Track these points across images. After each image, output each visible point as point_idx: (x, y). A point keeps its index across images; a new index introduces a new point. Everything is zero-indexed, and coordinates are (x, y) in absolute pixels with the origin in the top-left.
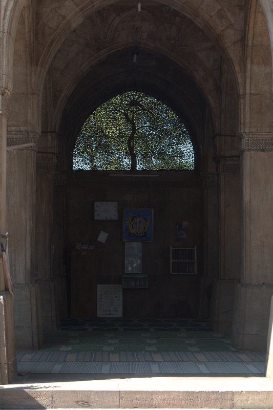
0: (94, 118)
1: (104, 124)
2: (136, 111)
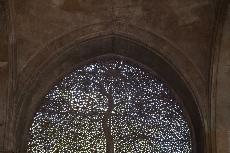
0: (59, 90)
1: (73, 98)
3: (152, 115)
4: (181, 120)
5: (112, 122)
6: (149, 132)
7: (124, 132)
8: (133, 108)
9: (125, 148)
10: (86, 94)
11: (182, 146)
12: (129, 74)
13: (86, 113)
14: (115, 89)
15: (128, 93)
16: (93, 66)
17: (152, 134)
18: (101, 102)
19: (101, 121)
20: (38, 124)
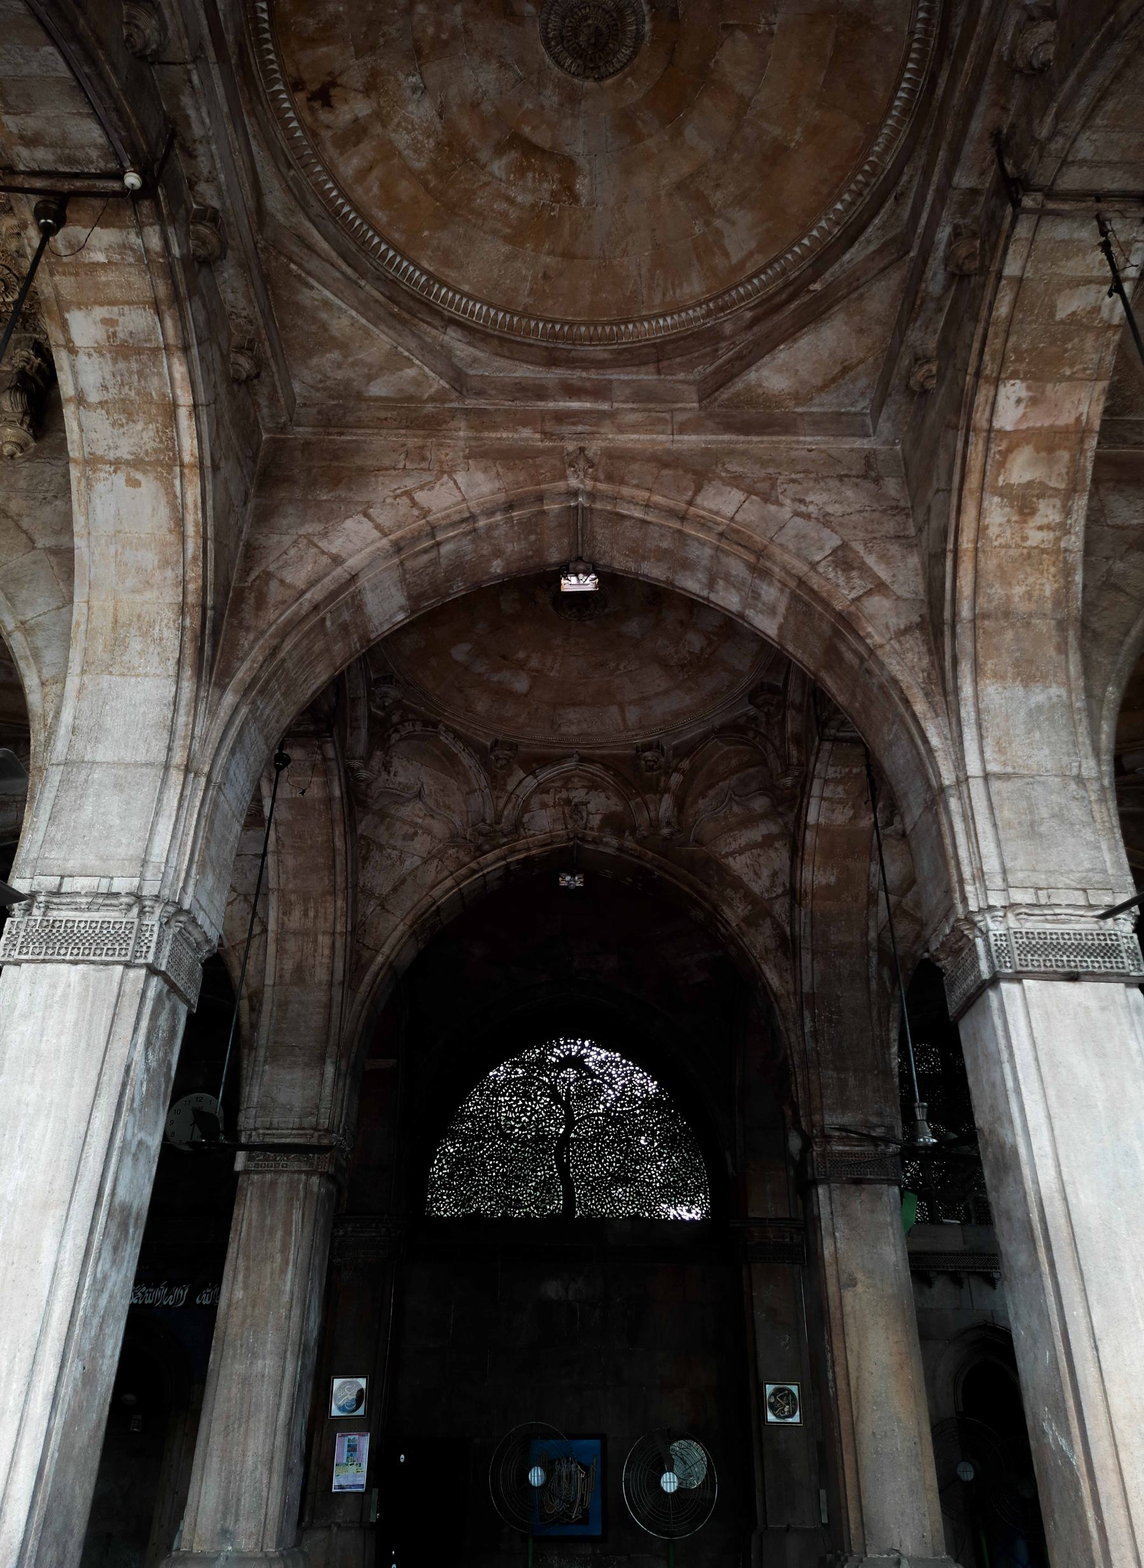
0: (481, 1095)
6: (636, 1171)
7: (593, 1172)
12: (602, 1064)
16: (537, 1051)
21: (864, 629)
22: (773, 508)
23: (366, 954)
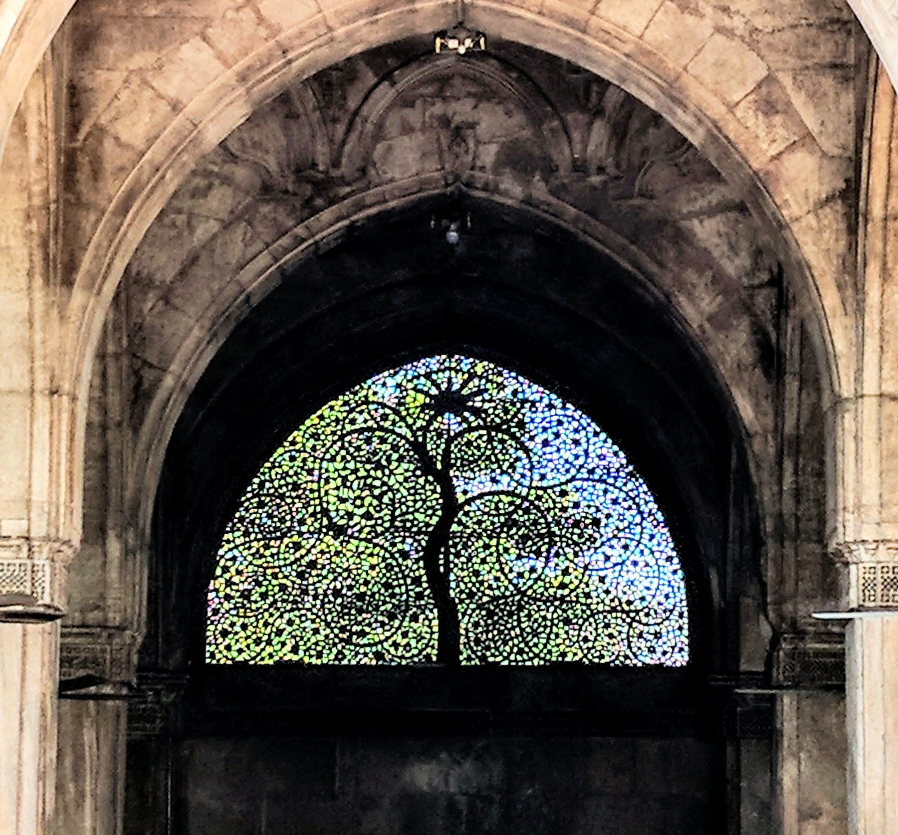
0: (293, 459)
2: (460, 434)
3: (572, 534)
4: (659, 544)
5: (452, 557)
8: (515, 511)
9: (494, 636)
10: (372, 473)
11: (658, 624)
13: (376, 532)
14: (459, 455)
15: (500, 467)
16: (391, 382)
17: (572, 591)
18: (418, 497)
19: (421, 554)
20: (233, 570)
21: (781, 193)
22: (690, 20)
23: (148, 375)
